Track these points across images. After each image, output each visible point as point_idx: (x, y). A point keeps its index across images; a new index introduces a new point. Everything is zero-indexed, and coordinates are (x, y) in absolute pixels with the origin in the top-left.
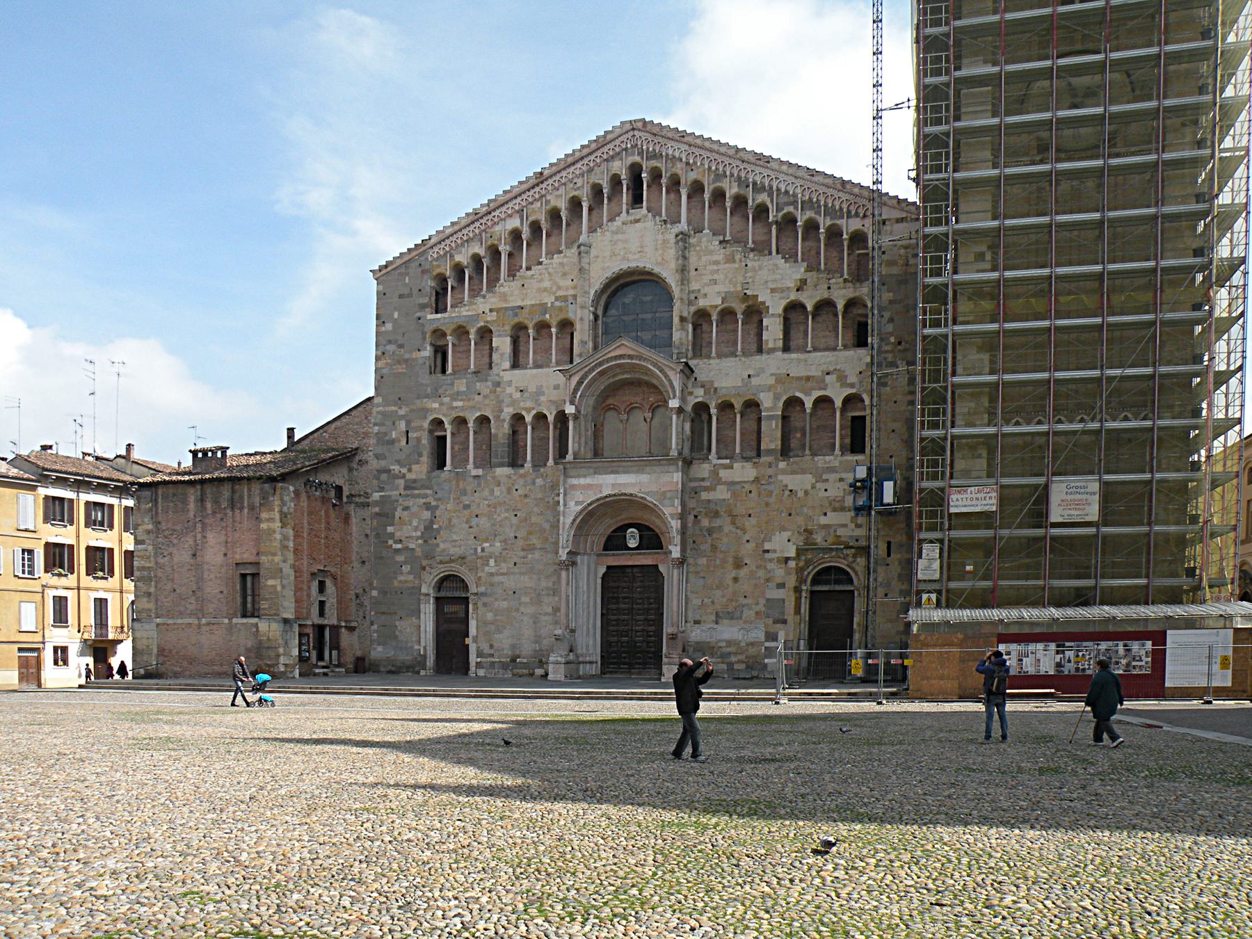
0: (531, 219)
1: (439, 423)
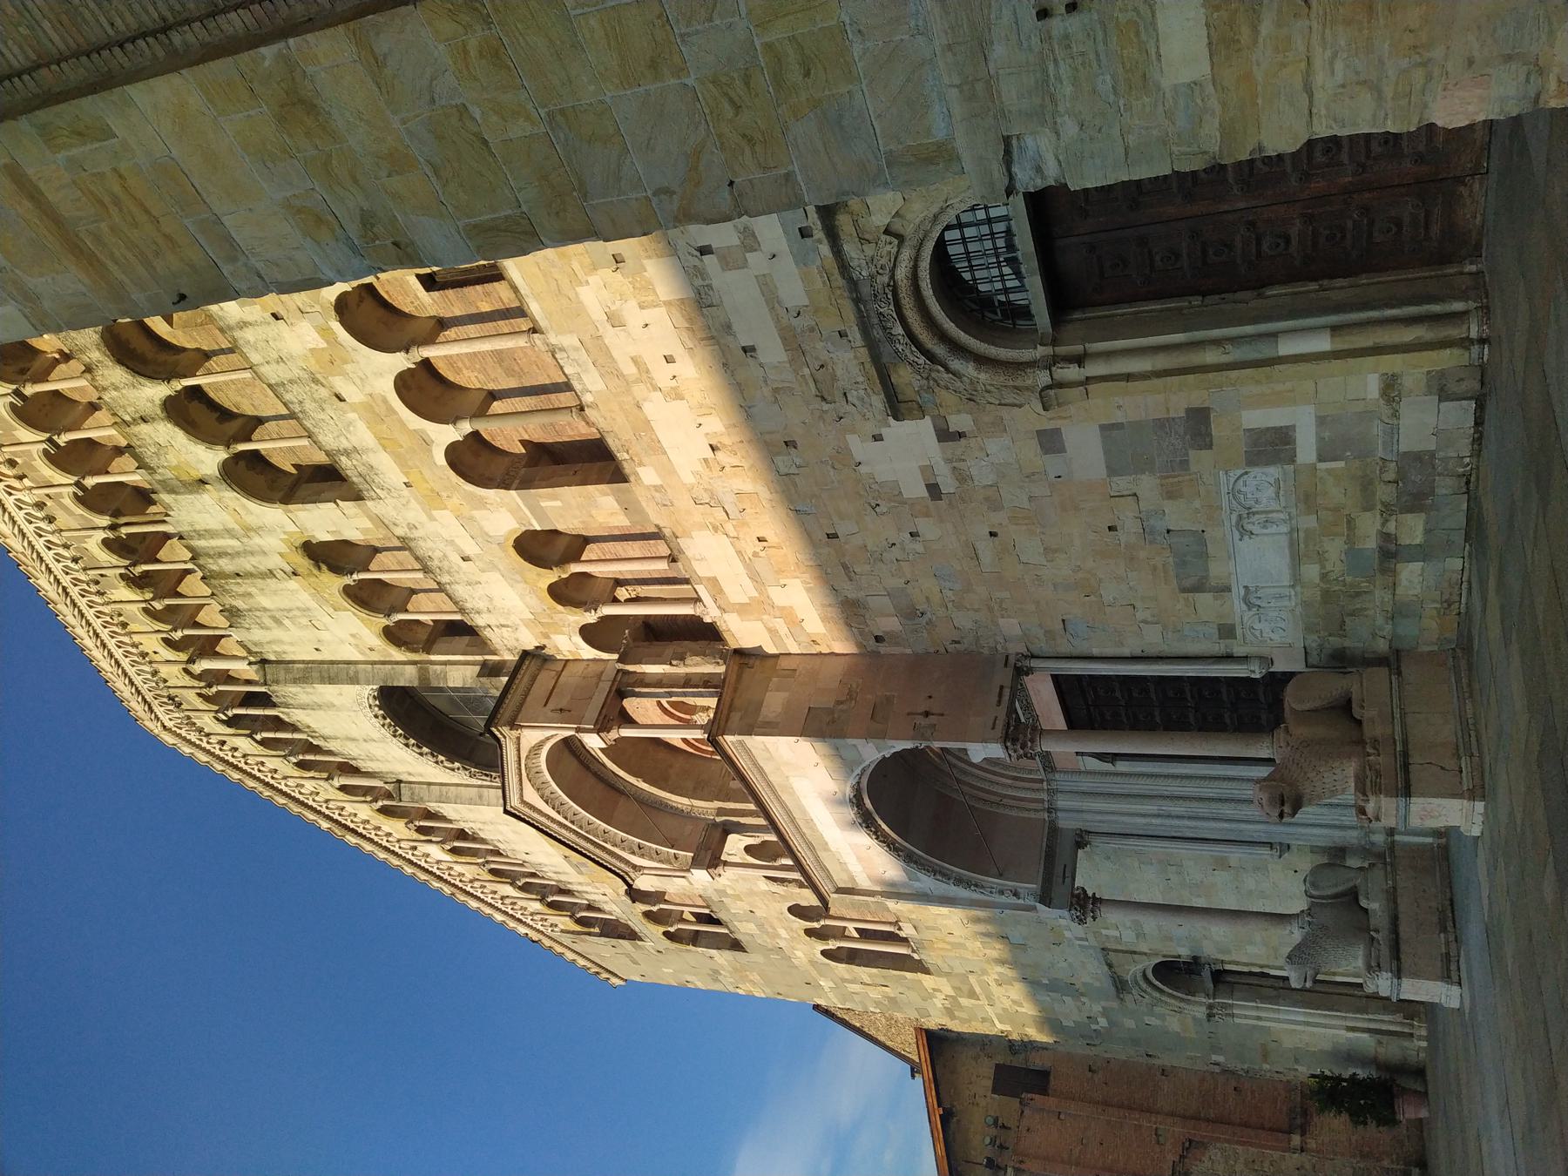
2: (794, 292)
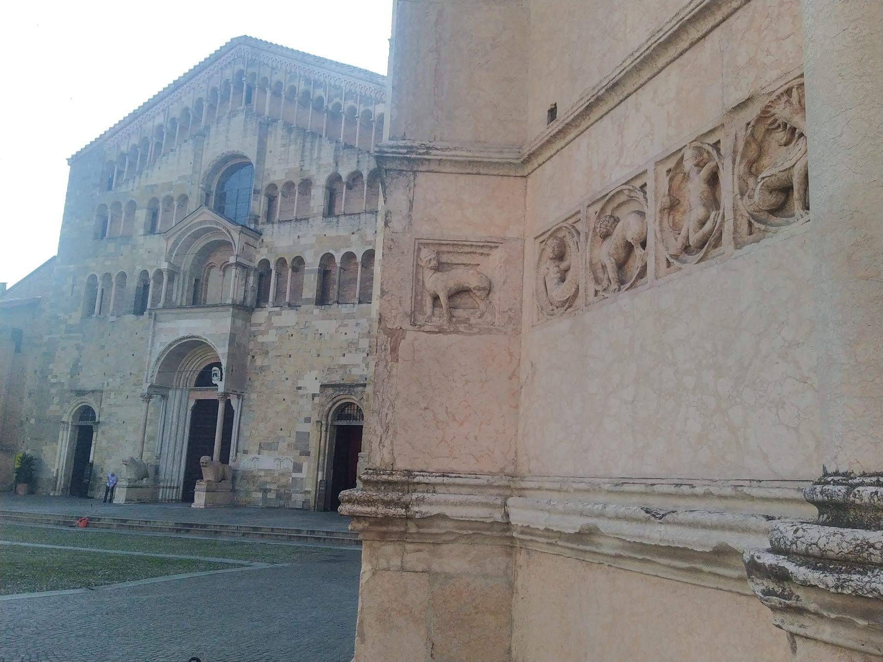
0: (171, 116)
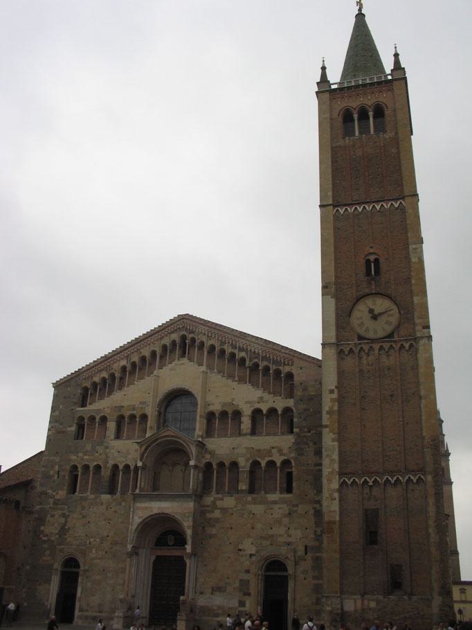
0: (132, 361)
1: (75, 467)
2: (281, 539)
